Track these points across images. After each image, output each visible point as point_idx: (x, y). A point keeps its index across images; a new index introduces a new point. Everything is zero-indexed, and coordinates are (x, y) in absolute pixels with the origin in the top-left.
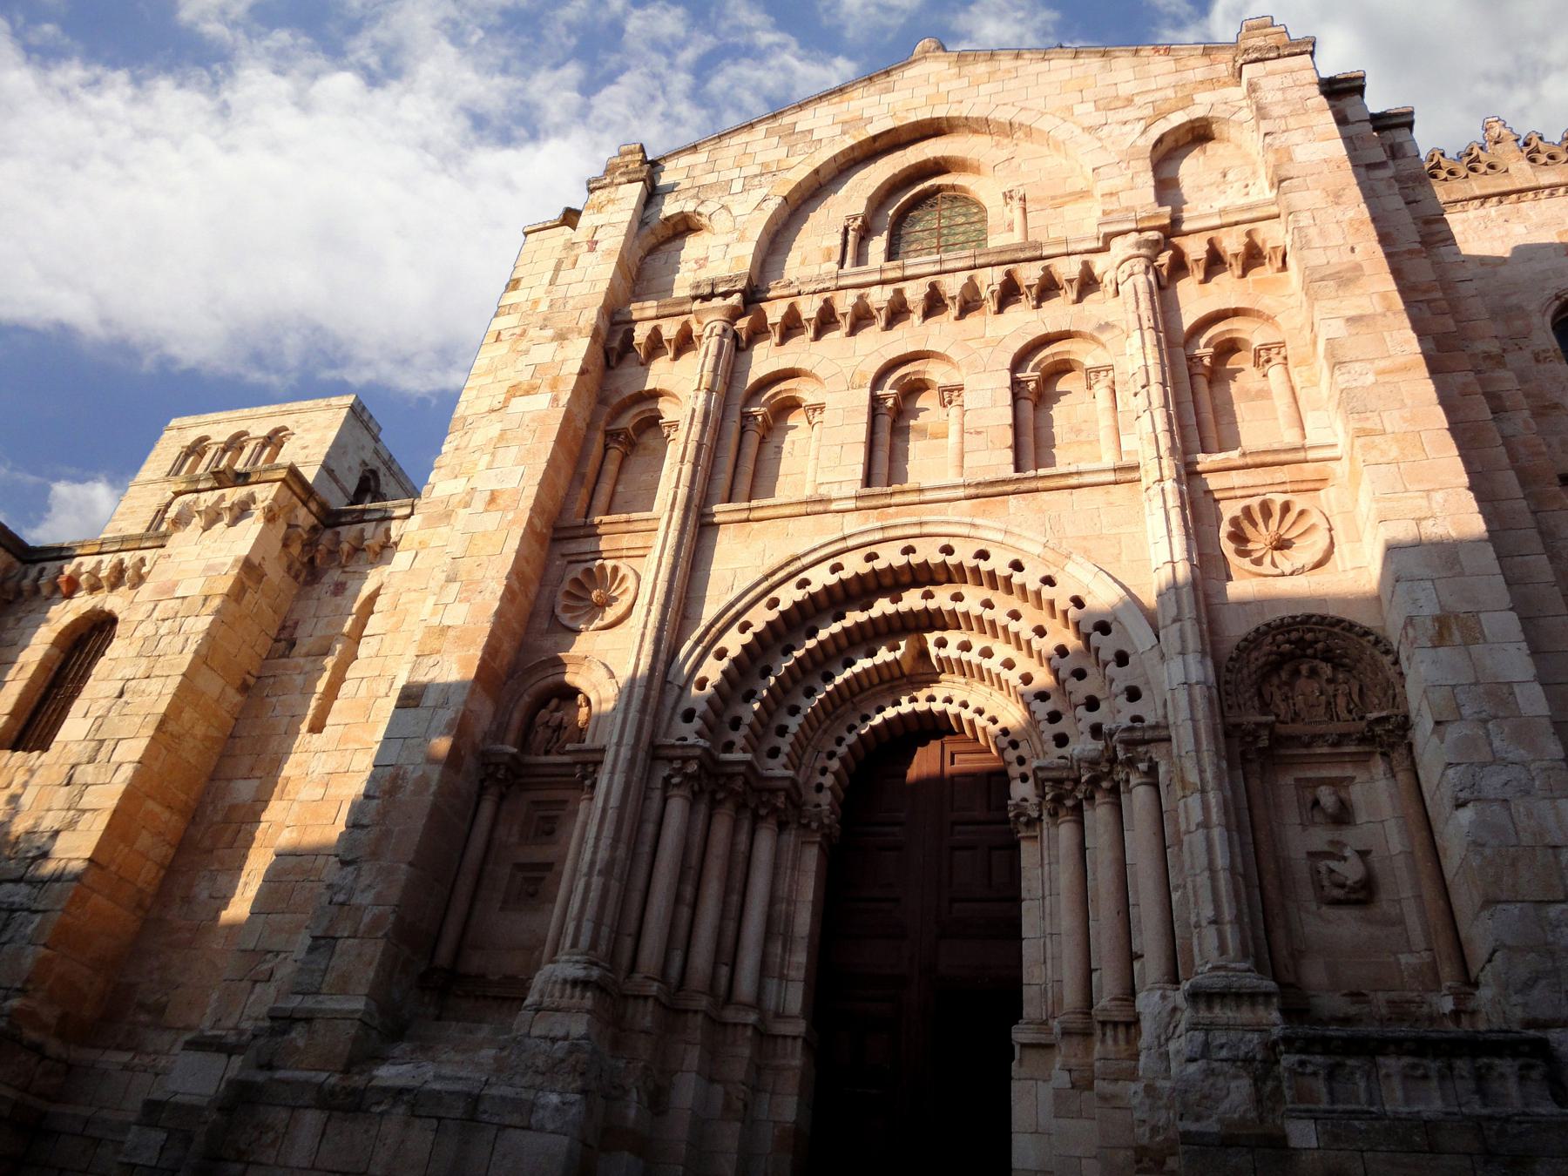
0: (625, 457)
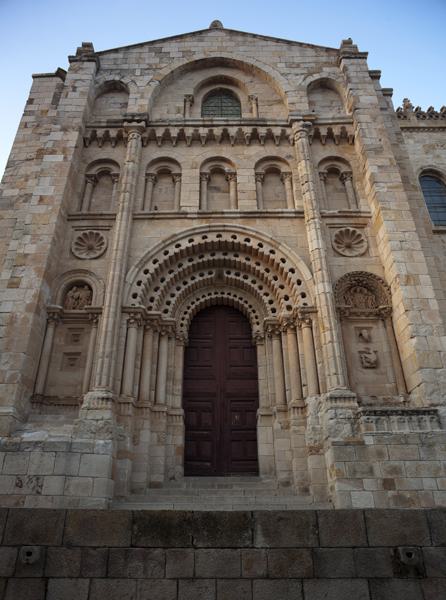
0: (94, 186)
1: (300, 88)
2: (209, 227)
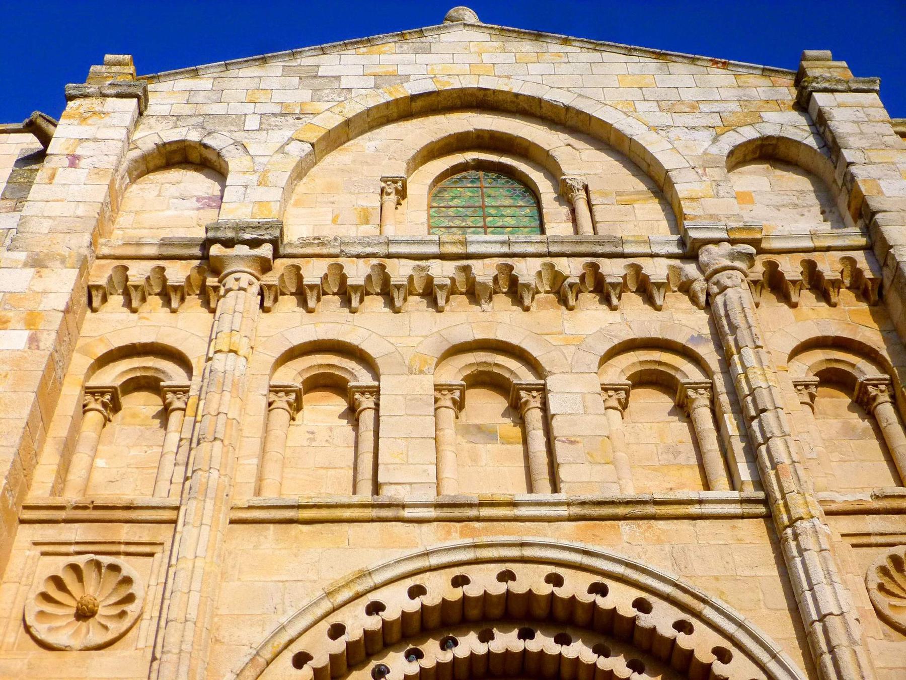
1: (707, 162)
2: (476, 546)
